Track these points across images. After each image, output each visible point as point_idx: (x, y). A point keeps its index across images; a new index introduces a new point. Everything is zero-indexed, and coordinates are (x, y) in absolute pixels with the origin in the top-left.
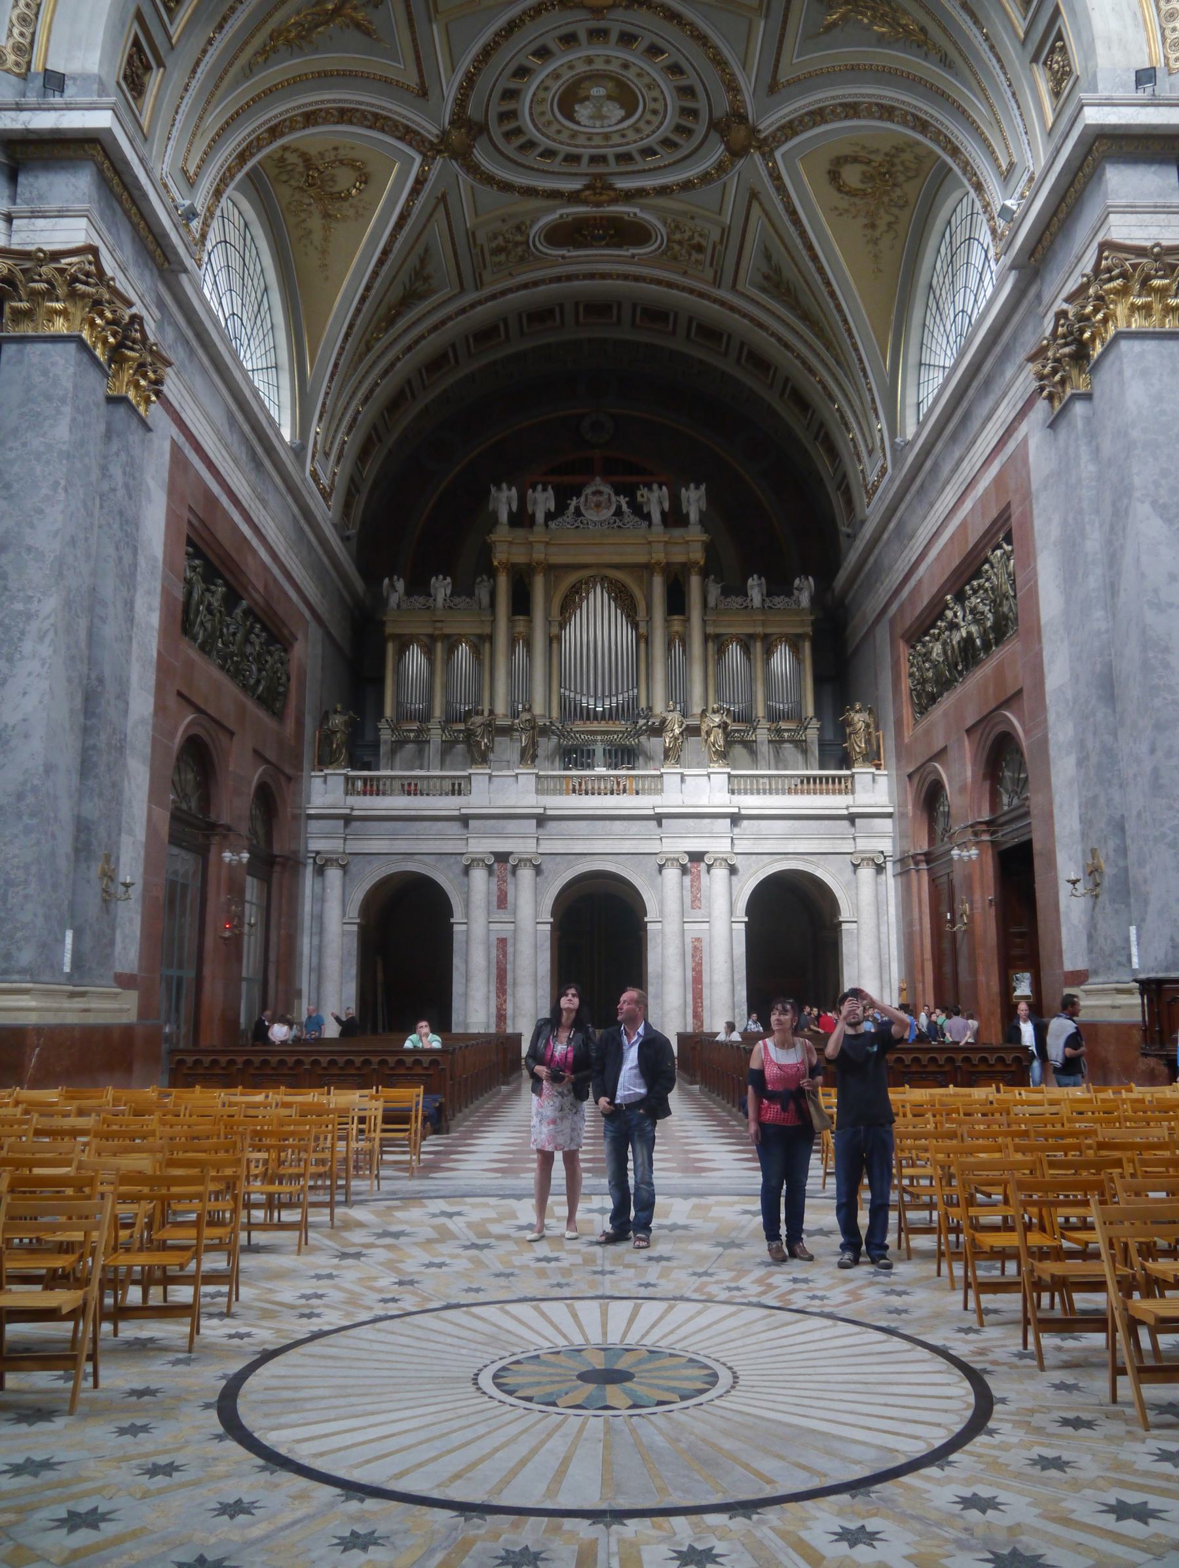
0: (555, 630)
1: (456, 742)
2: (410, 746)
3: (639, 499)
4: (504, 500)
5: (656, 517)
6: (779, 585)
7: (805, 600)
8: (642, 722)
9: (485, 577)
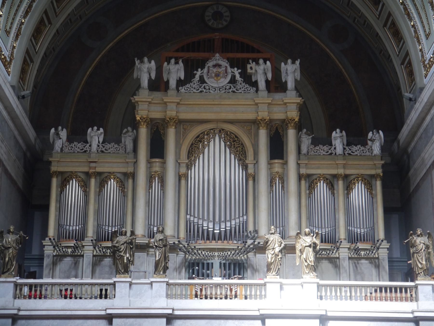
0: (183, 170)
1: (105, 256)
2: (68, 259)
3: (249, 71)
4: (146, 70)
5: (262, 85)
7: (376, 148)
8: (250, 242)
9: (129, 129)
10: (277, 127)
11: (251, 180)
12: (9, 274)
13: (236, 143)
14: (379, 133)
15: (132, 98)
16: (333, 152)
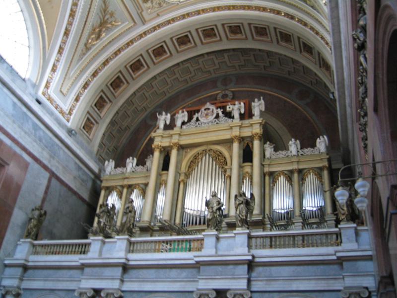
0: (182, 177)
3: (228, 109)
6: (308, 142)
14: (323, 137)
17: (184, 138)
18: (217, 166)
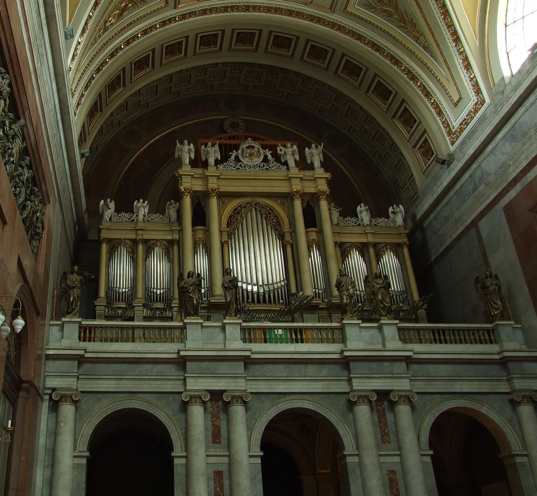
0: (225, 238)
4: (186, 150)
9: (172, 201)
10: (308, 201)
11: (289, 247)
12: (73, 314)
13: (271, 215)
15: (176, 172)
16: (361, 223)
17: (222, 182)
18: (269, 227)
